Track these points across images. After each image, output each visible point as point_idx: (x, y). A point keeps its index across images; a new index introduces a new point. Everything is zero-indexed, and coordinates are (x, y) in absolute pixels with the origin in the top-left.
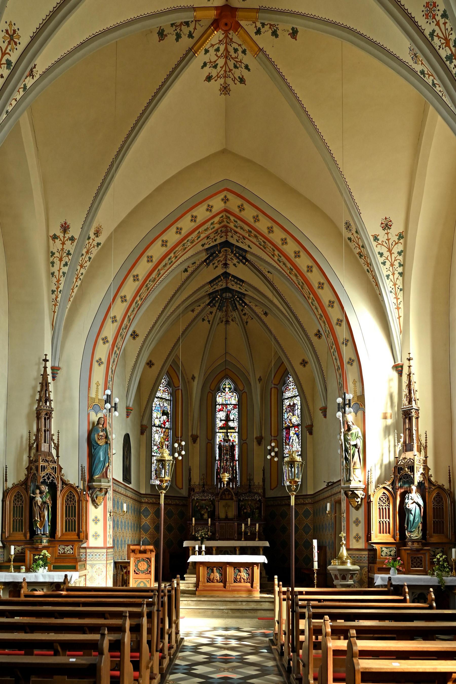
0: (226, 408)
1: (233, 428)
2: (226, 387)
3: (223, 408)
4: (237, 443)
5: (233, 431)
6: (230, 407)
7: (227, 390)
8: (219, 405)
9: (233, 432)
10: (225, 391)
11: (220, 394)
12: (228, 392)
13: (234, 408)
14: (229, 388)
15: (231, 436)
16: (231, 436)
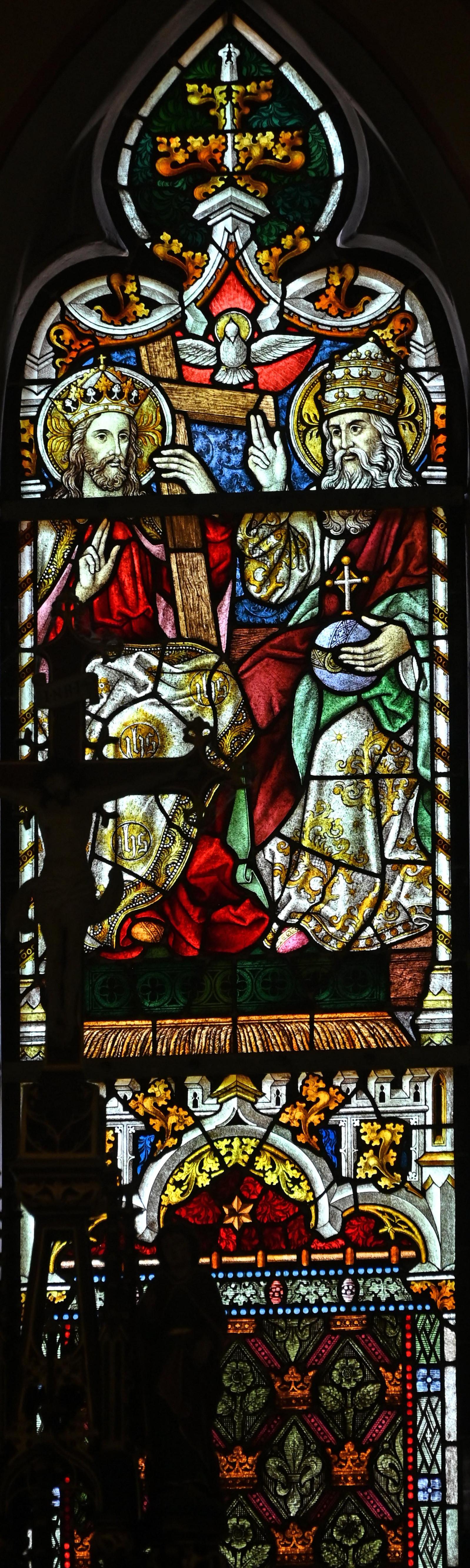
0: (224, 575)
1: (357, 976)
2: (204, 172)
3: (158, 580)
4: (439, 1254)
5: (360, 1030)
6: (283, 569)
7: (225, 215)
8: (76, 517)
9: (364, 1062)
10: (199, 236)
11: (83, 307)
12: (255, 263)
13: (382, 568)
14: (258, 173)
15: (322, 1141)
16: (322, 1141)
